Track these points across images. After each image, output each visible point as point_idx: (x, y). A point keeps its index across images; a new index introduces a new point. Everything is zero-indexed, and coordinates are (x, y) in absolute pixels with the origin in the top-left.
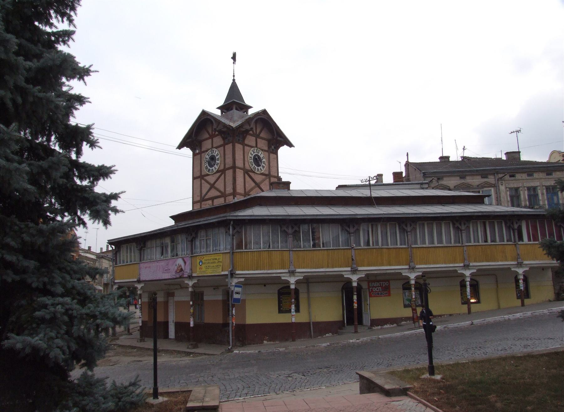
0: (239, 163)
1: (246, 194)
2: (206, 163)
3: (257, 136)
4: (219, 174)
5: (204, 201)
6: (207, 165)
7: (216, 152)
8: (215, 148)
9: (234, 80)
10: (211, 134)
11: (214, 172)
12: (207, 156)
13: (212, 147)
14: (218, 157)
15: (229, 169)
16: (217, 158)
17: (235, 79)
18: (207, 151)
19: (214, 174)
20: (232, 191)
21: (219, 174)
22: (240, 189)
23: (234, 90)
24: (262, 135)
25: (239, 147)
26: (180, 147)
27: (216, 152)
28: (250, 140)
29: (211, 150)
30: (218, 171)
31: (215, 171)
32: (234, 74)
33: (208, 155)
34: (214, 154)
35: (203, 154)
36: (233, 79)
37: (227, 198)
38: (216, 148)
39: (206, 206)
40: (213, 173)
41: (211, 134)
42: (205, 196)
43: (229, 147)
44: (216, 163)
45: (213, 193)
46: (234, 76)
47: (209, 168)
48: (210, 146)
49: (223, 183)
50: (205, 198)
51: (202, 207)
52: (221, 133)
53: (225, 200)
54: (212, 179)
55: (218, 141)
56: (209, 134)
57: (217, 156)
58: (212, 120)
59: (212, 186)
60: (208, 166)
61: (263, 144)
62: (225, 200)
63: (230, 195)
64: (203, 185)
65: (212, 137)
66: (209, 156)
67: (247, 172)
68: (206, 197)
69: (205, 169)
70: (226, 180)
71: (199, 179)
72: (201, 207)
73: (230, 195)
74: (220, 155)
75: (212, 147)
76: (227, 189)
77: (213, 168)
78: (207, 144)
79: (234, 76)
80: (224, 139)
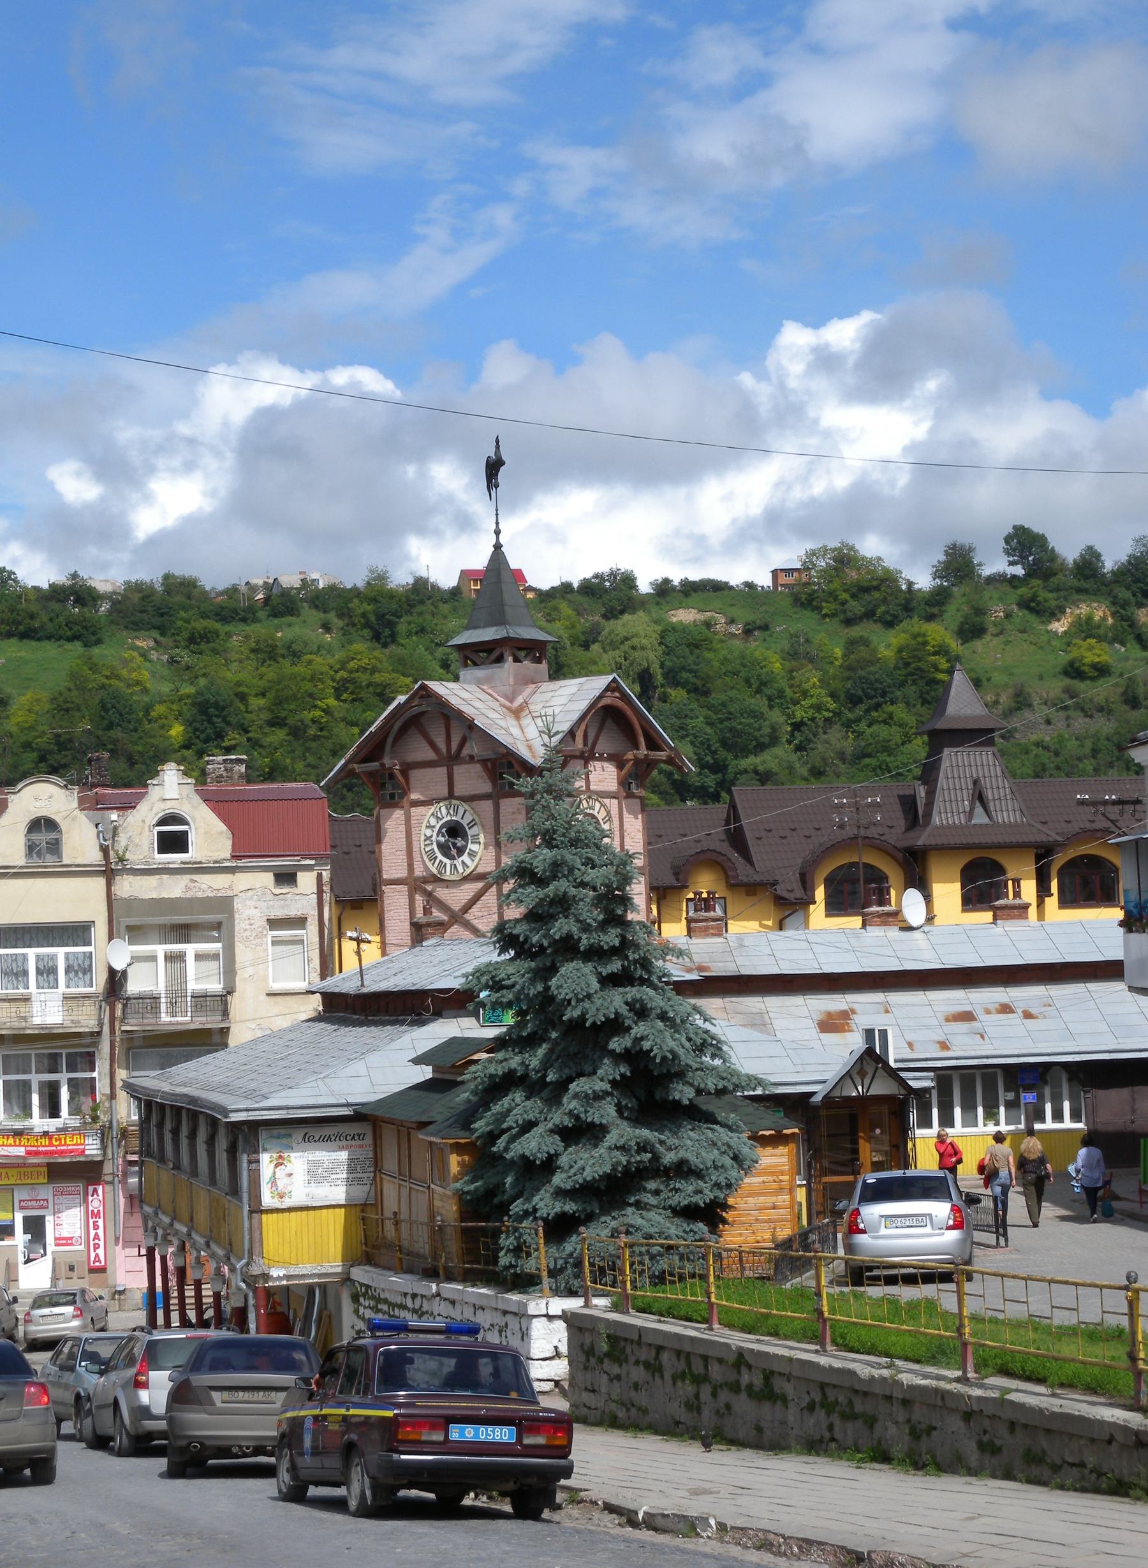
4: (480, 885)
6: (435, 846)
8: (459, 798)
9: (498, 547)
13: (451, 795)
17: (502, 540)
21: (480, 885)
24: (599, 748)
27: (464, 815)
29: (447, 802)
32: (497, 523)
33: (438, 818)
35: (413, 810)
40: (453, 878)
41: (444, 750)
47: (440, 857)
48: (445, 792)
55: (471, 779)
56: (433, 745)
60: (436, 850)
66: (441, 823)
69: (427, 861)
71: (404, 888)
75: (451, 795)
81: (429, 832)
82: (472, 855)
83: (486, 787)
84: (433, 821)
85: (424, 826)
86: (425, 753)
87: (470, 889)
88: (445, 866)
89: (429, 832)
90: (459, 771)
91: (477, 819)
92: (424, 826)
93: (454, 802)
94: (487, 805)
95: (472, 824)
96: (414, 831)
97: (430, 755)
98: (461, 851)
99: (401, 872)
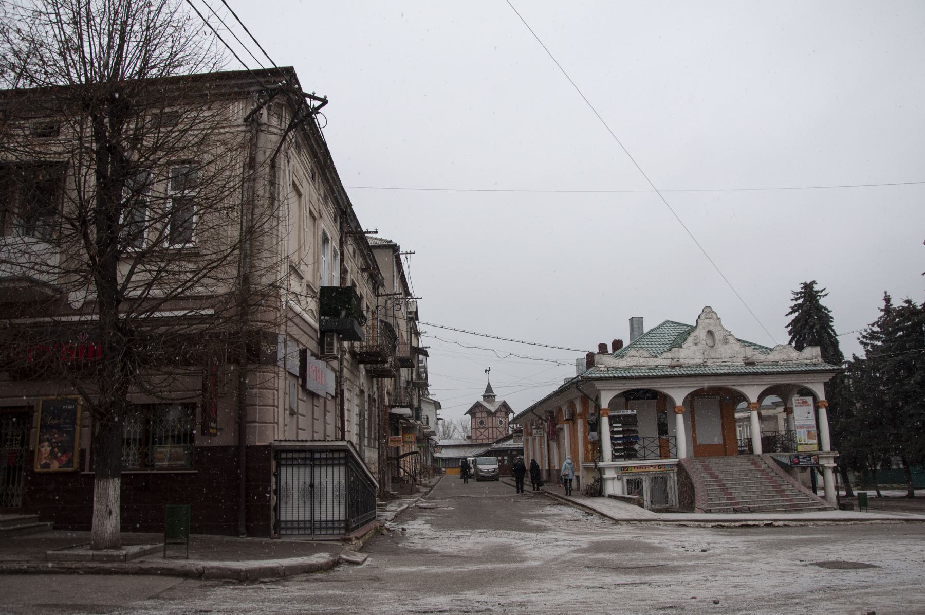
0: (494, 426)
1: (497, 438)
3: (501, 411)
12: (479, 420)
22: (495, 436)
23: (489, 388)
25: (494, 418)
26: (465, 414)
28: (498, 414)
30: (484, 428)
43: (490, 419)
45: (482, 437)
52: (486, 412)
55: (484, 414)
61: (503, 414)
65: (482, 412)
67: (497, 428)
78: (478, 415)
87: (484, 430)
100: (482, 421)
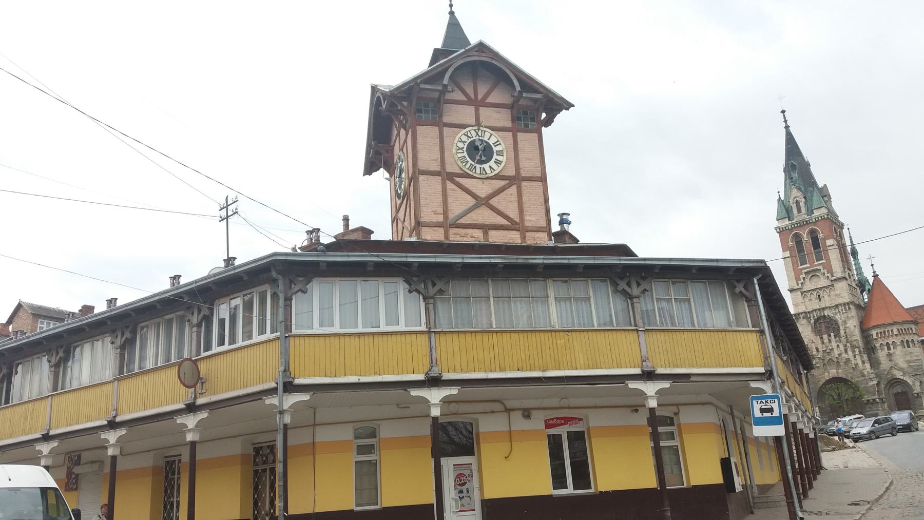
2: (460, 151)
4: (502, 183)
5: (455, 227)
6: (465, 154)
7: (491, 138)
9: (452, 13)
10: (472, 96)
11: (487, 176)
14: (499, 148)
15: (530, 179)
16: (495, 149)
18: (463, 126)
19: (488, 178)
20: (543, 223)
30: (498, 177)
31: (490, 174)
33: (468, 137)
34: (486, 139)
35: (445, 129)
36: (450, 10)
37: (528, 234)
38: (493, 129)
39: (465, 239)
41: (472, 96)
42: (461, 218)
44: (493, 159)
45: (484, 216)
46: (451, 6)
47: (470, 162)
48: (474, 123)
49: (516, 205)
50: (457, 222)
51: (451, 239)
53: (524, 238)
54: (483, 189)
57: (495, 146)
58: (508, 72)
59: (483, 202)
62: (524, 238)
63: (539, 230)
64: (449, 192)
65: (477, 103)
66: (470, 140)
68: (462, 221)
69: (459, 163)
70: (525, 198)
72: (447, 237)
73: (539, 230)
74: (505, 144)
76: (527, 218)
77: (486, 166)
79: (451, 6)
80: (515, 119)
81: (461, 145)
82: (498, 162)
83: (509, 124)
84: (464, 138)
85: (457, 139)
86: (458, 95)
88: (475, 167)
89: (461, 145)
90: (482, 110)
91: (501, 141)
92: (457, 139)
93: (481, 128)
94: (509, 135)
95: (497, 144)
96: (447, 141)
97: (463, 98)
98: (481, 162)
99: (436, 167)
100: (473, 149)
